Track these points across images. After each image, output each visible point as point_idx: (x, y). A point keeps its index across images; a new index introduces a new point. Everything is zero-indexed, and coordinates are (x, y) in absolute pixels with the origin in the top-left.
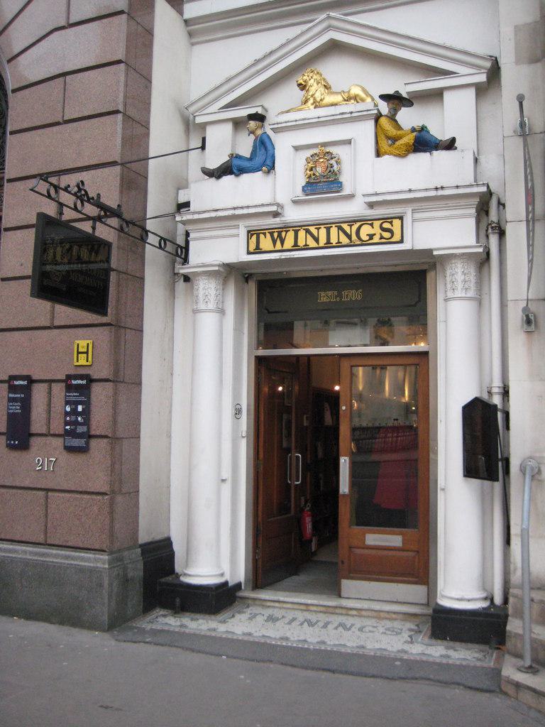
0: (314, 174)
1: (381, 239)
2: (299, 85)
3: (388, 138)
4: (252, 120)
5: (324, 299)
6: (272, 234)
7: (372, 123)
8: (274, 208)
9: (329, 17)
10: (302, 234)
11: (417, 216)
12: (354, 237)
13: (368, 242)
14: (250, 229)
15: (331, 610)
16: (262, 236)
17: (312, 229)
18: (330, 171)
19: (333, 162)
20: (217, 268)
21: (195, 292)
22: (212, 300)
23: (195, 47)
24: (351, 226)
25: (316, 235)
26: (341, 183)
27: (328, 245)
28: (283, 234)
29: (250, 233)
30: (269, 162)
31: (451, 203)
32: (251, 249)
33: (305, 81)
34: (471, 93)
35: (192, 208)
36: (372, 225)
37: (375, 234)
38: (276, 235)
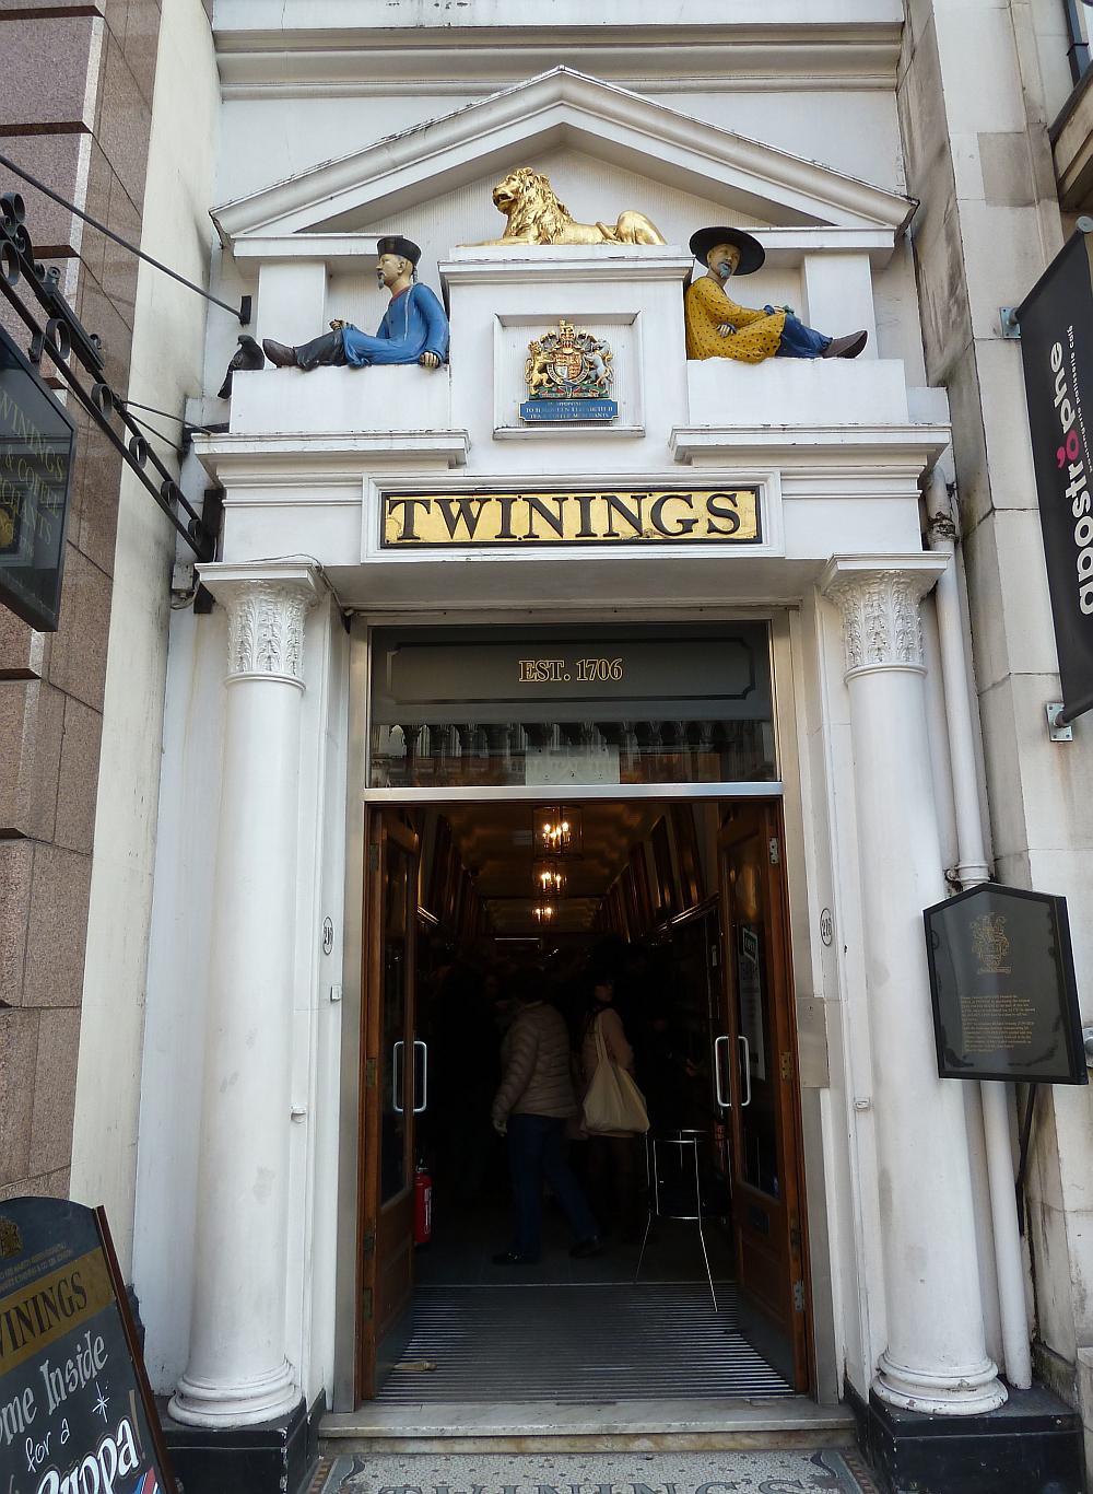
0: (550, 381)
1: (709, 532)
2: (498, 199)
3: (717, 320)
4: (394, 252)
5: (535, 677)
6: (445, 505)
8: (457, 444)
9: (562, 76)
10: (520, 509)
12: (647, 524)
15: (581, 1445)
16: (419, 509)
17: (546, 500)
18: (588, 377)
19: (596, 357)
20: (305, 574)
21: (235, 637)
22: (282, 659)
23: (232, 105)
24: (639, 499)
25: (555, 513)
27: (586, 538)
28: (474, 507)
29: (389, 499)
30: (440, 347)
31: (866, 464)
33: (516, 192)
34: (863, 266)
36: (687, 500)
37: (697, 521)
38: (455, 508)
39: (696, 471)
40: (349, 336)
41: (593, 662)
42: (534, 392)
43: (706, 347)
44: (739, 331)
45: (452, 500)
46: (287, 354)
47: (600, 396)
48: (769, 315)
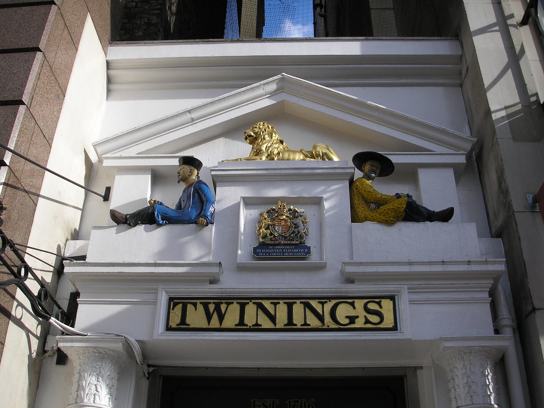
1: (365, 323)
6: (206, 306)
7: (347, 183)
8: (215, 270)
10: (251, 309)
11: (416, 297)
13: (348, 327)
14: (173, 295)
16: (190, 307)
17: (267, 304)
18: (293, 232)
19: (299, 221)
24: (323, 304)
25: (273, 312)
26: (309, 248)
27: (290, 327)
28: (223, 307)
29: (173, 301)
32: (173, 325)
33: (256, 133)
34: (450, 174)
35: (88, 260)
36: (352, 304)
37: (358, 317)
38: (212, 307)
39: (357, 287)
40: (157, 207)
41: (298, 402)
42: (261, 240)
43: (363, 216)
44: (382, 207)
45: (210, 303)
46: (122, 218)
47: (301, 243)
48: (398, 198)
